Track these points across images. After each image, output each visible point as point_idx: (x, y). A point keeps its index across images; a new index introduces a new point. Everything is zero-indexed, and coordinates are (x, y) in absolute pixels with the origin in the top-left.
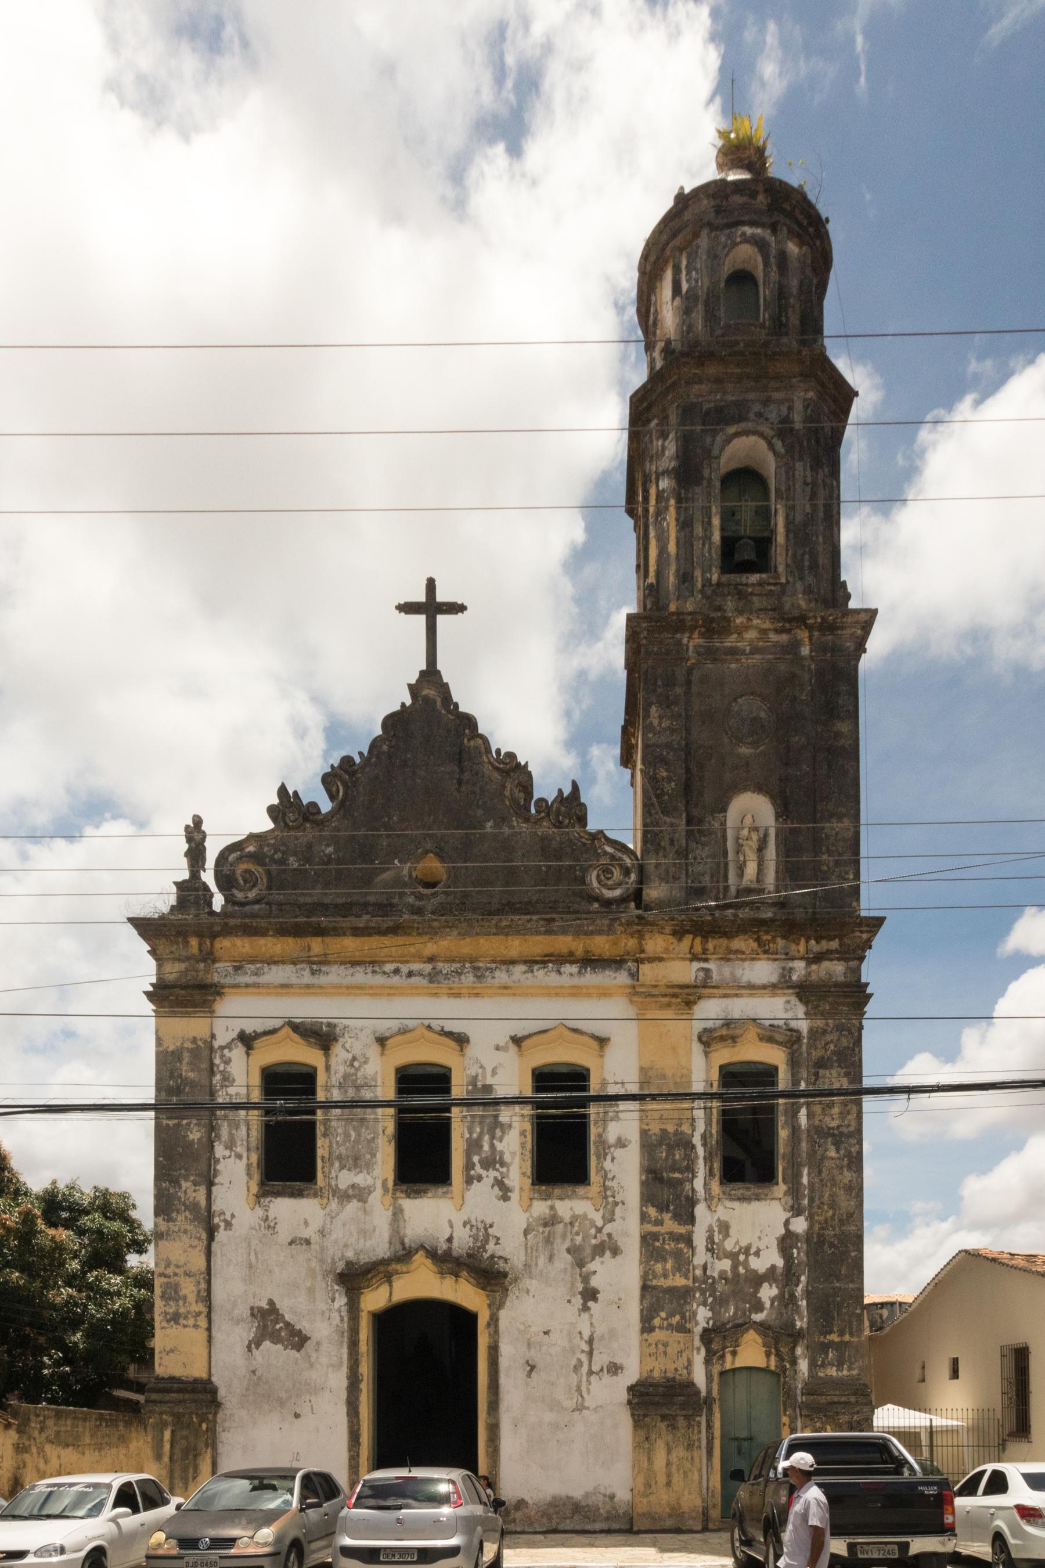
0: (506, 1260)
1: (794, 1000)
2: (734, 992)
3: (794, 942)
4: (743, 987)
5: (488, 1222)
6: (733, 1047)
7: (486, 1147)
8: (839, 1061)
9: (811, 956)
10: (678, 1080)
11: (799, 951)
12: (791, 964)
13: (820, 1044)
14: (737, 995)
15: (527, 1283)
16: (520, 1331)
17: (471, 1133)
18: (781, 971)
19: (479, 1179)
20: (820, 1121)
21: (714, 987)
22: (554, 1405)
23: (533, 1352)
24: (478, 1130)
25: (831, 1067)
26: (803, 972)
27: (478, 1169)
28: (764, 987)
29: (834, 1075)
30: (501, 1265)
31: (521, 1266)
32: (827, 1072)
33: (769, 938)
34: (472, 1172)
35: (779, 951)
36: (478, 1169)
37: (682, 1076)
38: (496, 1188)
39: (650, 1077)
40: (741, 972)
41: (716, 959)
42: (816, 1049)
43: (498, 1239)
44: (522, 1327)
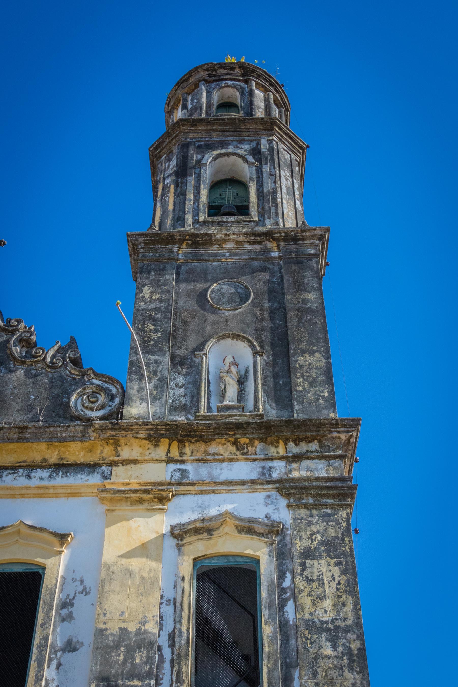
1: (274, 493)
2: (211, 488)
3: (272, 444)
4: (221, 483)
6: (209, 539)
8: (328, 551)
9: (290, 455)
10: (145, 575)
11: (278, 453)
12: (270, 464)
13: (305, 535)
14: (214, 492)
18: (261, 470)
20: (311, 614)
21: (189, 484)
25: (320, 557)
26: (284, 470)
28: (243, 483)
29: (323, 565)
32: (315, 562)
33: (247, 441)
35: (258, 453)
37: (151, 570)
39: (113, 572)
40: (218, 471)
41: (194, 461)
42: (301, 539)
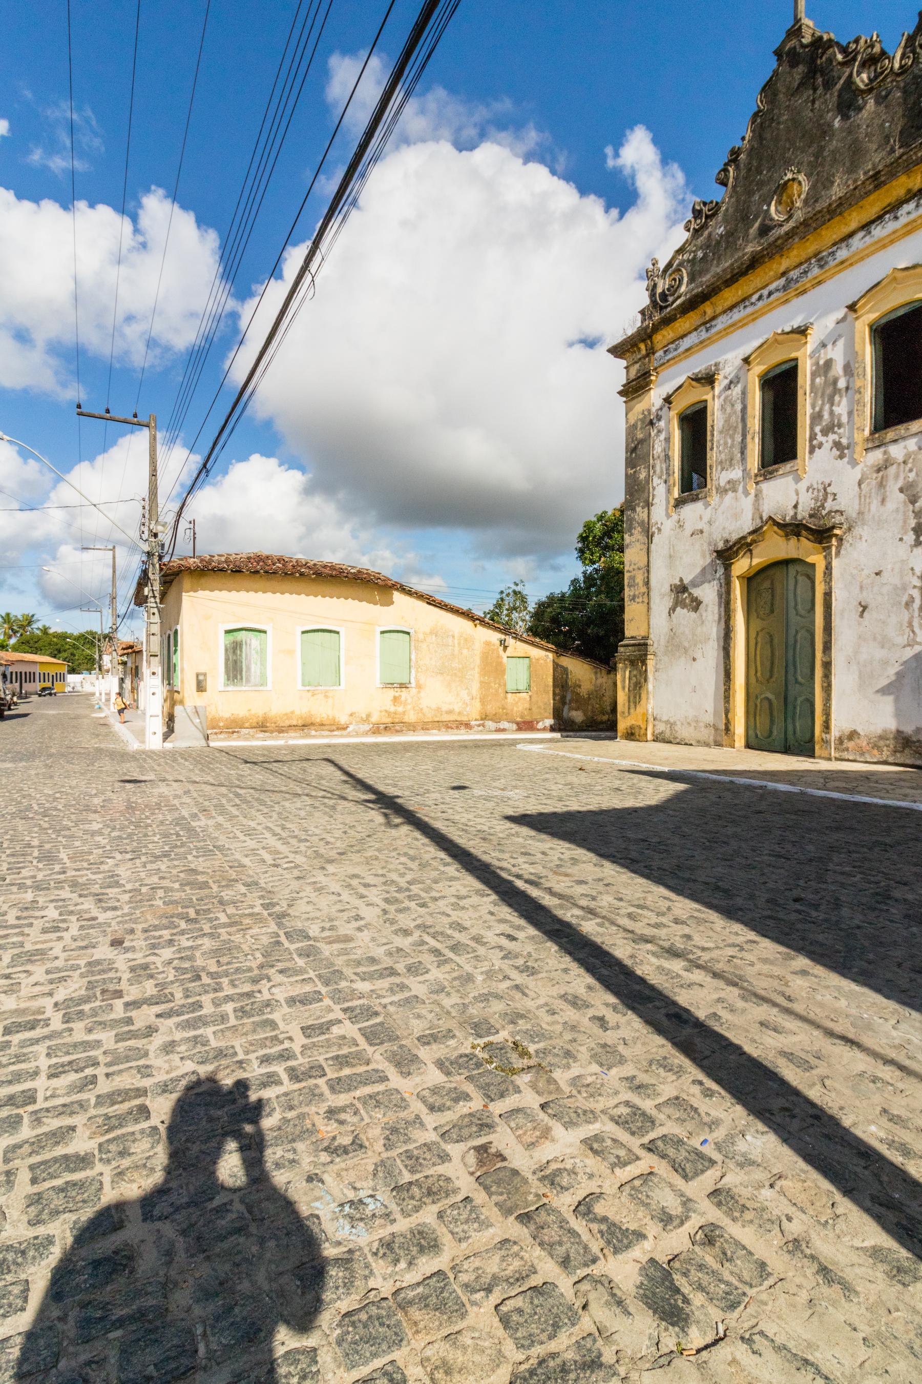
0: (841, 513)
5: (827, 482)
7: (826, 416)
15: (857, 531)
16: (853, 576)
17: (813, 406)
19: (820, 446)
22: (884, 642)
23: (865, 593)
24: (820, 402)
27: (820, 438)
30: (838, 519)
31: (854, 515)
34: (815, 442)
36: (820, 438)
38: (834, 449)
43: (835, 495)
44: (855, 572)
